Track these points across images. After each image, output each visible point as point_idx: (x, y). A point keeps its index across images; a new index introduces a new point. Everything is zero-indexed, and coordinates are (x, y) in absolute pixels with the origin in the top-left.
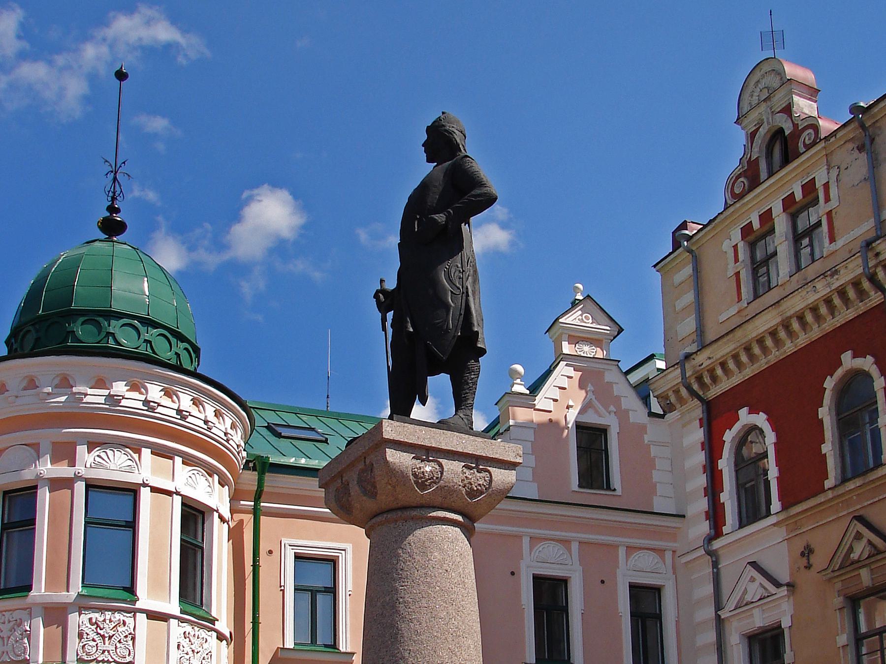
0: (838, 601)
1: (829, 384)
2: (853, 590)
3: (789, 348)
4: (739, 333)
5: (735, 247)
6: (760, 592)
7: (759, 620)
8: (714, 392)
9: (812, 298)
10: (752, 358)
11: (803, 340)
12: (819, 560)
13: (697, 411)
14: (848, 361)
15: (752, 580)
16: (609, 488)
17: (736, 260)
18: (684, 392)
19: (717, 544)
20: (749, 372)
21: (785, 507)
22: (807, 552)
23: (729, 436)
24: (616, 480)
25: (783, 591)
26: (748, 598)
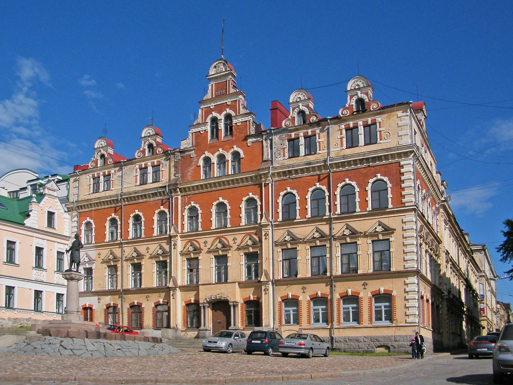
8: (81, 211)
16: (54, 228)
22: (99, 254)
24: (56, 226)
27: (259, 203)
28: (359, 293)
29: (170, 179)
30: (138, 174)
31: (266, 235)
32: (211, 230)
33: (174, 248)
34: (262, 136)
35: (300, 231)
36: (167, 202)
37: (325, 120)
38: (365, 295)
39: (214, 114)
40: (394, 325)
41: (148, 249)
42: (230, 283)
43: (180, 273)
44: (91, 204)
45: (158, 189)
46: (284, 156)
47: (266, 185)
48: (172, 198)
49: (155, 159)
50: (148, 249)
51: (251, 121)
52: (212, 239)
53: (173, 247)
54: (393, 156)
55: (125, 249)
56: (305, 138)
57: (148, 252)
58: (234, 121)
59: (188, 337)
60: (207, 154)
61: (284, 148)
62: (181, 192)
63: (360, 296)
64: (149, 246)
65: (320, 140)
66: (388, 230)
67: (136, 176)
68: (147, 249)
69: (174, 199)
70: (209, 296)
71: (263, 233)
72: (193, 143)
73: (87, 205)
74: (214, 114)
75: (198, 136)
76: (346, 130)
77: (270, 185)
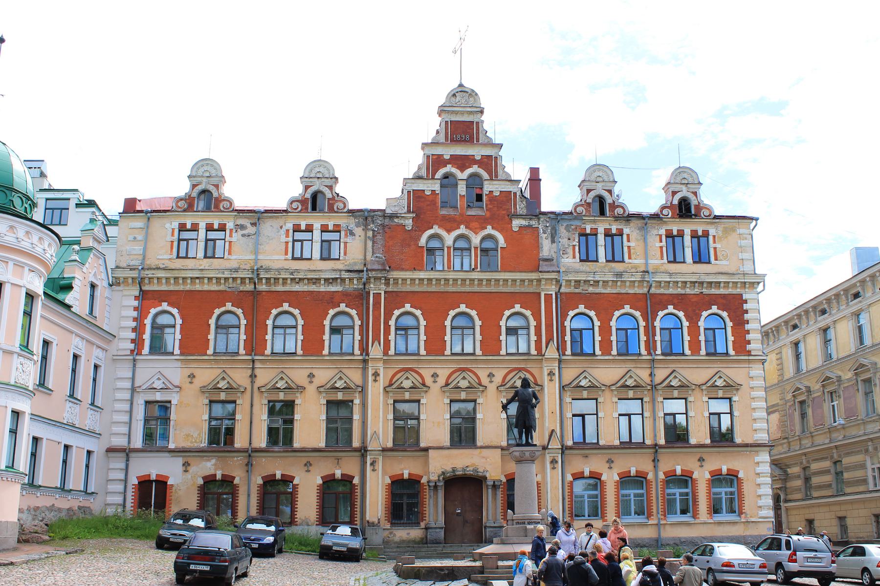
0: (207, 402)
1: (217, 312)
3: (198, 287)
5: (173, 229)
7: (158, 397)
8: (146, 288)
11: (206, 287)
12: (199, 382)
13: (137, 293)
14: (229, 306)
15: (159, 379)
17: (173, 235)
19: (138, 357)
20: (172, 288)
21: (182, 354)
22: (192, 376)
23: (153, 311)
25: (178, 389)
26: (154, 386)
29: (365, 259)
30: (290, 239)
32: (444, 355)
33: (375, 381)
34: (539, 219)
36: (359, 299)
37: (639, 216)
39: (449, 168)
41: (311, 376)
42: (482, 447)
44: (175, 278)
45: (343, 273)
46: (574, 257)
49: (330, 218)
50: (311, 376)
51: (518, 194)
52: (447, 372)
53: (371, 378)
55: (257, 372)
56: (606, 235)
57: (311, 382)
58: (488, 187)
59: (397, 539)
60: (436, 229)
61: (574, 246)
62: (387, 284)
64: (315, 372)
65: (629, 244)
67: (287, 243)
68: (309, 376)
72: (409, 207)
73: (167, 278)
75: (419, 197)
76: (667, 237)
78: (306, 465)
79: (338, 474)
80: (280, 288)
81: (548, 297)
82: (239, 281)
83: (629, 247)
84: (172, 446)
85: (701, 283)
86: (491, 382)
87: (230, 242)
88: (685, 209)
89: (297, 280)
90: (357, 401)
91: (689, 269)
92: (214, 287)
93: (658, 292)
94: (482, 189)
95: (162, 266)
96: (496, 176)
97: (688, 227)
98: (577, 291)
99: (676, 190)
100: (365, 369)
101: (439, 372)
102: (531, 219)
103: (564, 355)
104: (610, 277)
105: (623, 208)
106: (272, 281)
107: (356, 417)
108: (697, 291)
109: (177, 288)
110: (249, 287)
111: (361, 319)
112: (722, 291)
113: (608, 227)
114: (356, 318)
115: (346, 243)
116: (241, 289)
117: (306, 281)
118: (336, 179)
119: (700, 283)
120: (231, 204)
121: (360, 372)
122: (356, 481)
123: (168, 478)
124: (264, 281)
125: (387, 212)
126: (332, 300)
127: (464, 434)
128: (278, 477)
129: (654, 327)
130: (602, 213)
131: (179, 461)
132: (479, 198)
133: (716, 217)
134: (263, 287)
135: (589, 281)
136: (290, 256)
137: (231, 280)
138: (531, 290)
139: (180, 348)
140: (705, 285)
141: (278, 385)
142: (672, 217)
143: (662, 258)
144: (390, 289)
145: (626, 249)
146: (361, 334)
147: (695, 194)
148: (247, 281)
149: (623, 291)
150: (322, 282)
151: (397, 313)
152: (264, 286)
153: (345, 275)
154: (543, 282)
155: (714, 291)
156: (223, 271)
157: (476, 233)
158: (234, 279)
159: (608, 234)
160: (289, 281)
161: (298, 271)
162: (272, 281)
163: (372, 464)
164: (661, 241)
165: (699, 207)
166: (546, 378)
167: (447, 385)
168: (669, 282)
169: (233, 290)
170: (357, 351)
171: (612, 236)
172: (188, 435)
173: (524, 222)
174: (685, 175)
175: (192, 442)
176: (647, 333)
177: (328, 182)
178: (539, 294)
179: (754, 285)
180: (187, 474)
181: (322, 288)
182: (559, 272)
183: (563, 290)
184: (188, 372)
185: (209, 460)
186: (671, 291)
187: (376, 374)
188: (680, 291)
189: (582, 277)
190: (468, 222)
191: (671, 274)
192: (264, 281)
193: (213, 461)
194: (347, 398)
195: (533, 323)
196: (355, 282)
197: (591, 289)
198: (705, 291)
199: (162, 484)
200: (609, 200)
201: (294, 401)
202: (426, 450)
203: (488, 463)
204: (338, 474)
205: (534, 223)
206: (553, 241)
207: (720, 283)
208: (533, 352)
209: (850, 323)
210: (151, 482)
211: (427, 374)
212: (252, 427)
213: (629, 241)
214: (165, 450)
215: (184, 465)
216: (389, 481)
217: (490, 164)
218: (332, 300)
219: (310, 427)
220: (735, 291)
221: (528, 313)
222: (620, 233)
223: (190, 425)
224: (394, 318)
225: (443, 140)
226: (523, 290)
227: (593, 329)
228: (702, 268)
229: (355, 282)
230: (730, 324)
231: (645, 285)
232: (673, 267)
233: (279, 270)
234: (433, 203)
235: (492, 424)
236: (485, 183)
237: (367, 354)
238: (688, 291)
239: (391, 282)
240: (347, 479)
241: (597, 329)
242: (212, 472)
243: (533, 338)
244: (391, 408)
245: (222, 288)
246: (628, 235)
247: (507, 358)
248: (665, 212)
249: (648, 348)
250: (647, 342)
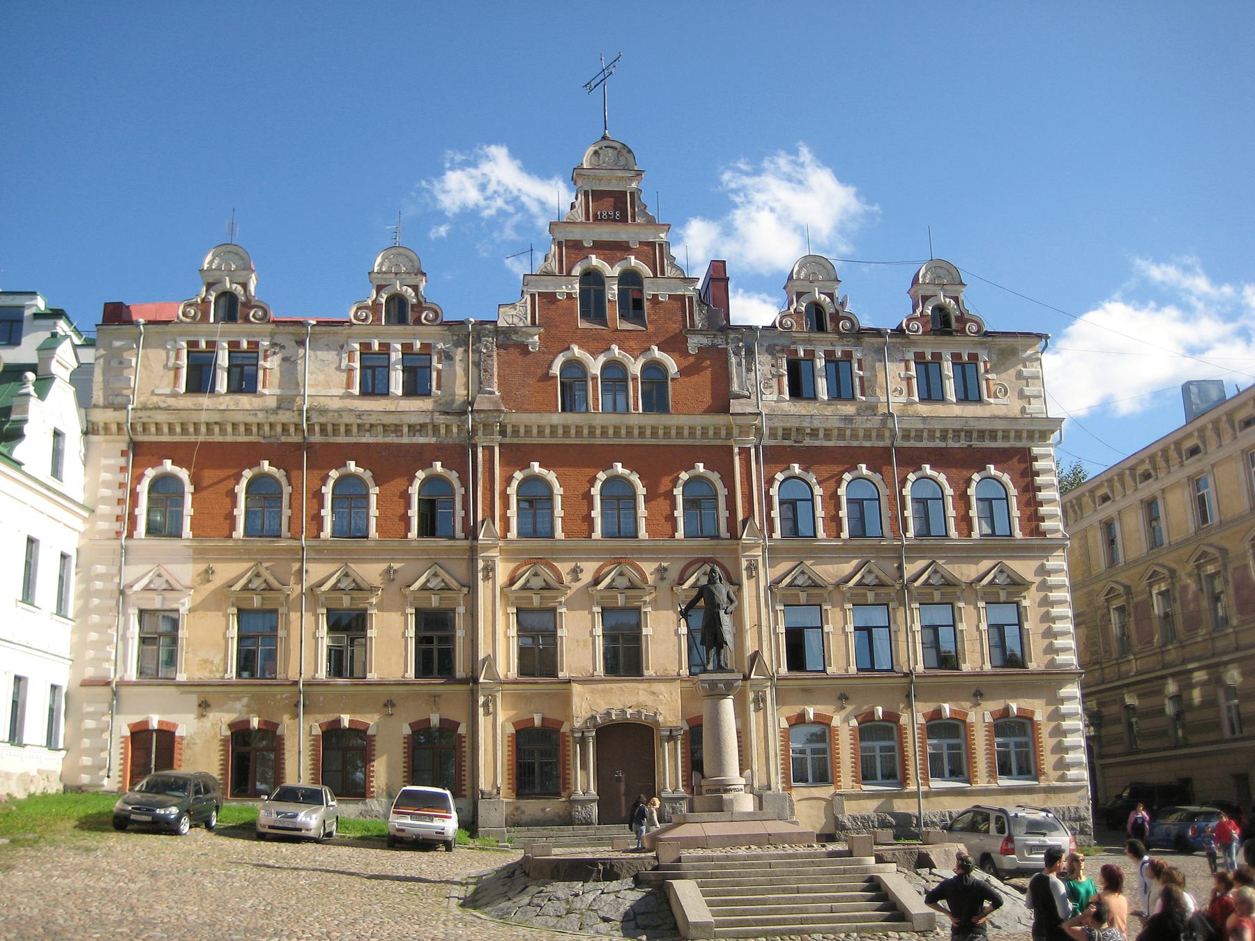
2: (245, 606)
3: (217, 438)
4: (184, 414)
6: (165, 586)
9: (250, 419)
10: (184, 431)
11: (229, 438)
12: (219, 580)
13: (124, 447)
18: (114, 428)
19: (130, 542)
20: (177, 439)
22: (209, 572)
27: (722, 492)
28: (966, 715)
30: (357, 365)
31: (752, 568)
33: (486, 578)
35: (829, 571)
37: (878, 333)
38: (980, 717)
40: (1043, 784)
43: (498, 642)
45: (436, 415)
47: (745, 452)
48: (475, 447)
49: (415, 336)
53: (480, 575)
54: (1018, 436)
60: (577, 351)
62: (503, 432)
63: (968, 720)
66: (1018, 584)
67: (350, 370)
69: (480, 450)
70: (602, 707)
71: (744, 564)
74: (595, 261)
77: (753, 451)
78: (385, 705)
79: (435, 720)
80: (341, 439)
81: (745, 452)
82: (279, 429)
83: (861, 378)
84: (181, 677)
85: (969, 433)
86: (662, 579)
87: (265, 369)
88: (944, 323)
89: (367, 427)
90: (461, 610)
91: (952, 410)
92: (242, 438)
93: (906, 444)
94: (641, 291)
95: (163, 405)
96: (663, 273)
97: (947, 349)
98: (787, 443)
99: (928, 293)
100: (473, 561)
101: (582, 565)
102: (715, 336)
103: (770, 536)
104: (835, 423)
105: (850, 320)
106: (330, 428)
107: (460, 633)
108: (963, 443)
109: (185, 439)
110: (295, 438)
111: (464, 483)
112: (1000, 444)
113: (830, 348)
114: (456, 484)
115: (439, 372)
116: (283, 439)
117: (380, 429)
118: (424, 274)
119: (966, 431)
120: (265, 312)
121: (465, 565)
122: (462, 730)
123: (175, 726)
124: (317, 428)
125: (500, 324)
126: (421, 456)
127: (624, 657)
128: (346, 724)
129: (903, 498)
130: (821, 327)
131: (194, 700)
132: (638, 304)
133: (987, 334)
134: (317, 438)
135: (804, 429)
136: (356, 390)
137: (267, 428)
138: (719, 442)
139: (192, 529)
140: (975, 435)
141: (342, 586)
142: (924, 333)
143: (910, 393)
144: (507, 440)
145: (857, 381)
146: (465, 507)
147: (956, 299)
148: (292, 429)
149: (855, 444)
150: (405, 429)
151: (518, 475)
152: (318, 435)
153: (440, 419)
154: (736, 431)
155: (988, 444)
156: (254, 412)
157: (636, 358)
158: (272, 425)
159: (829, 356)
160: (355, 429)
161: (369, 413)
162: (330, 428)
163: (486, 705)
164: (907, 369)
165: (962, 319)
166: (744, 573)
167: (596, 582)
168: (922, 431)
169: (272, 440)
170: (459, 533)
171: (836, 362)
172: (206, 661)
173: (705, 341)
174: (941, 272)
175: (211, 672)
176: (892, 506)
177: (412, 280)
178: (731, 448)
179: (1044, 436)
180: (204, 719)
181: (405, 440)
182: (760, 414)
183: (766, 441)
184: (202, 567)
185: (239, 699)
186: (925, 444)
187: (490, 570)
188: (939, 444)
189: (794, 423)
190: (622, 338)
191: (924, 418)
192: (317, 428)
193: (245, 700)
194: (445, 605)
195: (722, 492)
196: (455, 430)
197: (808, 442)
198: (976, 444)
199: (167, 737)
200: (829, 310)
201: (366, 610)
202: (569, 681)
203: (659, 699)
204: (435, 720)
205: (720, 341)
206: (749, 370)
207: (996, 431)
208: (723, 532)
209: (1186, 493)
210: (150, 732)
211: (564, 568)
212: (307, 648)
213: (860, 368)
214: (170, 682)
215: (200, 706)
216: (511, 730)
217: (656, 254)
218: (421, 456)
219: (391, 648)
220: (1018, 445)
221: (715, 477)
222: (848, 356)
223: (210, 646)
224: (515, 484)
225: (581, 218)
226: (705, 442)
227: (812, 500)
228: (970, 410)
229: (455, 430)
230: (1013, 491)
231: (887, 434)
232: (924, 409)
233: (339, 412)
234: (573, 312)
235: (665, 637)
236: (646, 283)
237: (476, 538)
238: (951, 444)
239: (509, 430)
240: (449, 727)
241: (818, 500)
242: (245, 717)
243: (723, 513)
244: (513, 619)
245: (252, 439)
246: (860, 362)
247: (686, 543)
248: (914, 325)
249: (894, 531)
250: (894, 519)
